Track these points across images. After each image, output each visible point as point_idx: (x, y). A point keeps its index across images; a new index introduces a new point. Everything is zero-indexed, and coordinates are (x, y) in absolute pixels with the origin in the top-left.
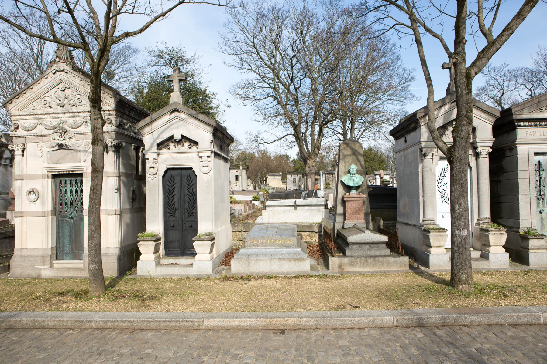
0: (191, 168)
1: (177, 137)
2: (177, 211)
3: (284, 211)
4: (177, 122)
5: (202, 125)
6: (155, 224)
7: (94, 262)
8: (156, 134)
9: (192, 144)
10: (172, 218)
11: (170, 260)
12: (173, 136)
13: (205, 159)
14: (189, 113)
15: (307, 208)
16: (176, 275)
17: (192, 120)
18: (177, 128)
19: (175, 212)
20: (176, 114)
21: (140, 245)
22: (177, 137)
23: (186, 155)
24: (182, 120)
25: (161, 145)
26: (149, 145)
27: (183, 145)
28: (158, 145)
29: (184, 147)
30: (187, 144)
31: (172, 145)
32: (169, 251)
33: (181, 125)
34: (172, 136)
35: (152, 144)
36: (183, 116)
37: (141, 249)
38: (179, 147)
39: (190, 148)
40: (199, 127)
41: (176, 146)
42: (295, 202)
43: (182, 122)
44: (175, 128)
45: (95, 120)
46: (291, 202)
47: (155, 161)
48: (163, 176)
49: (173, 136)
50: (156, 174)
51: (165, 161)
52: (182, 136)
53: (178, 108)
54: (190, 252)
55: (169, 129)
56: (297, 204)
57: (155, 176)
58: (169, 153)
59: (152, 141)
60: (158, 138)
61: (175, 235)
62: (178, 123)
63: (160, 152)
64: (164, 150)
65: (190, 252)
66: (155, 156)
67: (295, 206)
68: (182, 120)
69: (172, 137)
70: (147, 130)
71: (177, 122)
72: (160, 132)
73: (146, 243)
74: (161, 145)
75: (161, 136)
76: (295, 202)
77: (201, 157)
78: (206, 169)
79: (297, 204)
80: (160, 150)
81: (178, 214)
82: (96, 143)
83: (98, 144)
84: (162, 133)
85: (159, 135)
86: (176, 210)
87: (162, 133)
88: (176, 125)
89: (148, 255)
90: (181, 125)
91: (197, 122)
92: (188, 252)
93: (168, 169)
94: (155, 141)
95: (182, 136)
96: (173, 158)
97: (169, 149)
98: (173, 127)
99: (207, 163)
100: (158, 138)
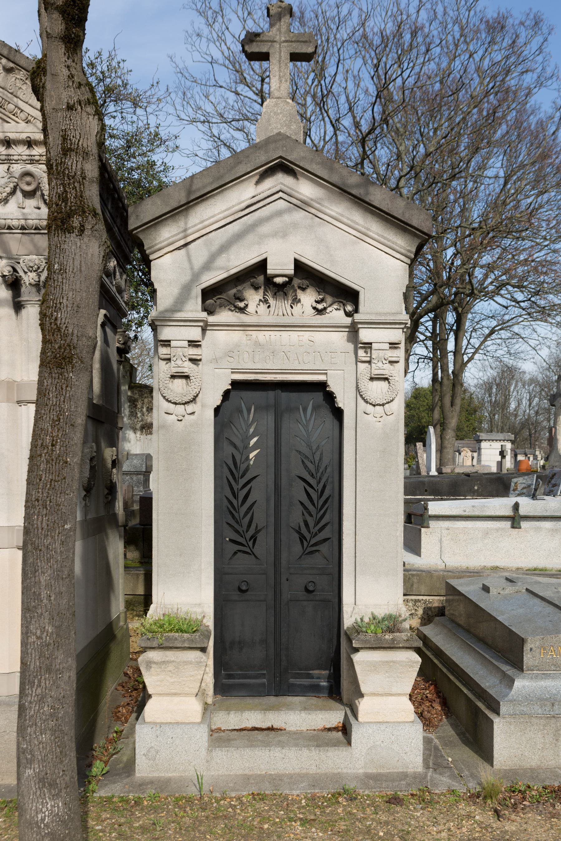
0: (321, 386)
1: (280, 266)
2: (261, 537)
3: (486, 533)
4: (279, 213)
5: (375, 227)
6: (185, 585)
7: (52, 785)
8: (199, 252)
9: (329, 299)
10: (243, 562)
11: (246, 714)
12: (265, 261)
13: (381, 352)
14: (335, 179)
15: (547, 525)
16: (302, 777)
17: (340, 209)
18: (283, 234)
19: (254, 538)
20: (281, 180)
21: (149, 664)
22: (280, 266)
23: (306, 336)
24: (303, 205)
25: (220, 295)
26: (175, 291)
27: (296, 300)
28: (208, 293)
29: (297, 309)
30: (308, 298)
31: (253, 298)
32: (230, 676)
33: (295, 226)
34: (263, 264)
35: (186, 290)
36: (306, 189)
37: (150, 680)
38: (279, 308)
39: (320, 312)
40: (363, 236)
41: (271, 301)
42: (516, 507)
43: (299, 215)
44: (275, 234)
45: (70, 108)
46: (500, 505)
47: (193, 352)
48: (217, 410)
49: (265, 261)
50: (194, 400)
51: (229, 353)
52: (299, 265)
53: (294, 156)
54: (306, 682)
55: (250, 237)
56: (522, 511)
57: (190, 408)
58: (244, 326)
59: (186, 277)
60: (207, 267)
61: (252, 621)
62: (287, 218)
63: (211, 319)
64: (225, 316)
65: (306, 682)
66: (195, 333)
67: (515, 519)
68: (303, 205)
69: (262, 265)
70: (167, 233)
71: (279, 213)
72: (215, 247)
73: (170, 655)
74: (220, 295)
75: (221, 261)
76: (516, 507)
77: (368, 346)
78: (376, 390)
79: (522, 511)
80: (211, 312)
81: (264, 546)
82: (76, 222)
83: (82, 230)
84: (224, 248)
85: (213, 257)
86: (257, 531)
87: (224, 248)
88: (276, 223)
89: (176, 699)
90: (295, 226)
91: (357, 217)
92: (298, 681)
93: (235, 384)
94: (196, 277)
95: (299, 265)
96: (257, 344)
97: (242, 310)
98: (265, 229)
99: (387, 369)
100: (207, 267)
